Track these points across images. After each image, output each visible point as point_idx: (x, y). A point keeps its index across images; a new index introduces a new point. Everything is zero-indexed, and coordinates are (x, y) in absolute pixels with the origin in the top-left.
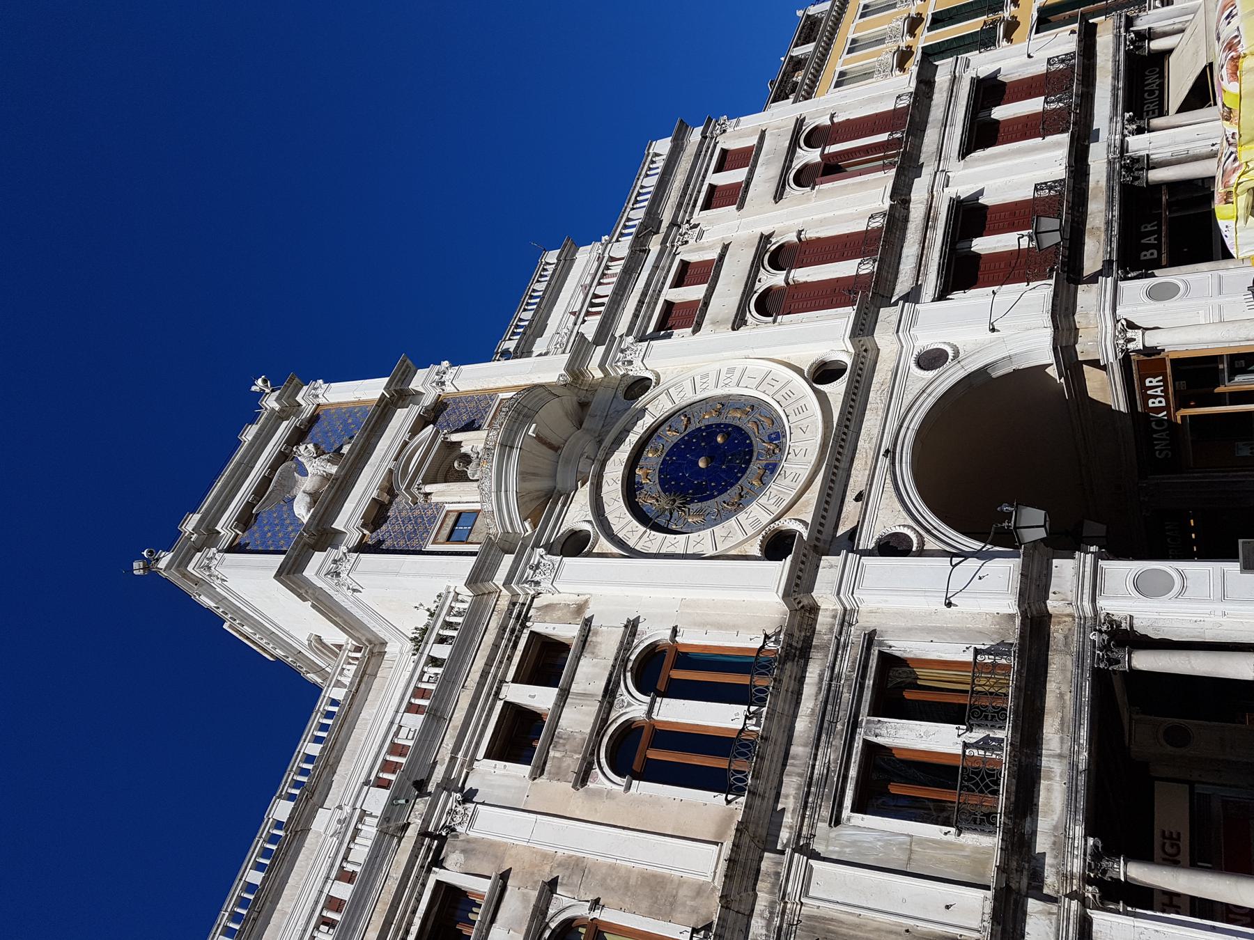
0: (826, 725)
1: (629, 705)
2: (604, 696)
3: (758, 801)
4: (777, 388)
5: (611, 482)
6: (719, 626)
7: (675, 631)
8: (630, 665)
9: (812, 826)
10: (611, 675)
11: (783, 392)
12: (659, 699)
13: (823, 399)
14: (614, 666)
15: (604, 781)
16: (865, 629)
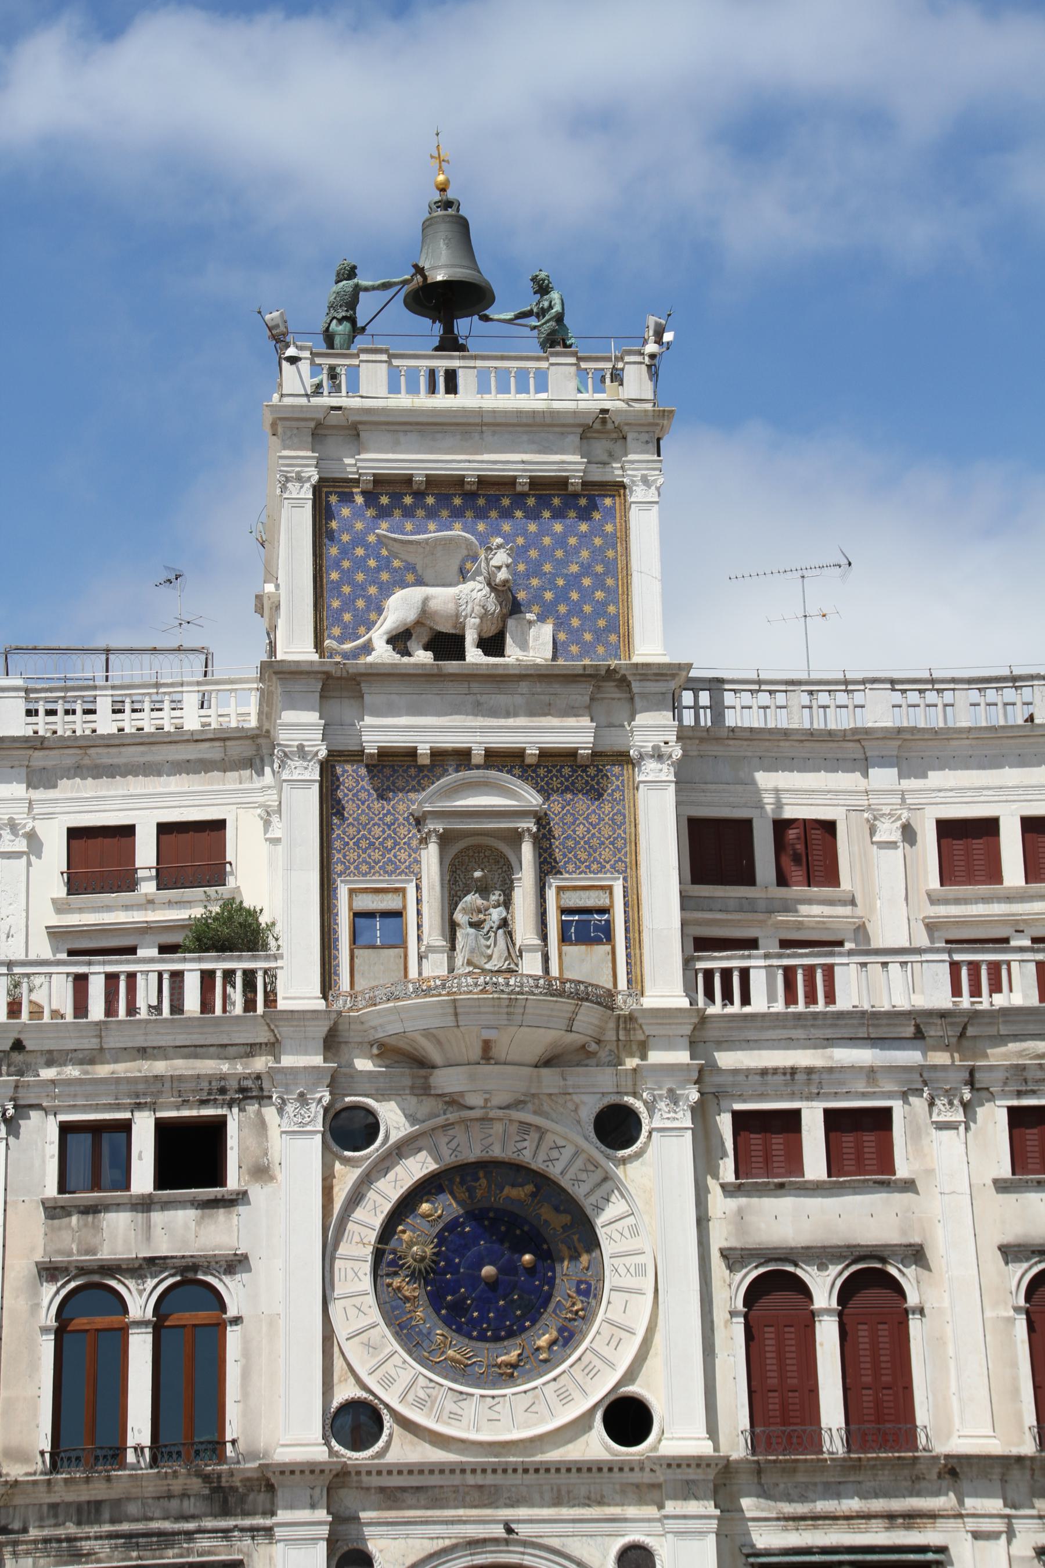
0: (134, 1540)
1: (140, 1292)
2: (145, 1259)
3: (43, 1488)
4: (606, 1351)
5: (453, 1145)
6: (246, 1375)
7: (237, 1320)
8: (190, 1275)
9: (27, 1553)
10: (172, 1257)
11: (596, 1362)
12: (150, 1330)
13: (580, 1425)
14: (183, 1257)
15: (50, 1296)
16: (249, 1555)
